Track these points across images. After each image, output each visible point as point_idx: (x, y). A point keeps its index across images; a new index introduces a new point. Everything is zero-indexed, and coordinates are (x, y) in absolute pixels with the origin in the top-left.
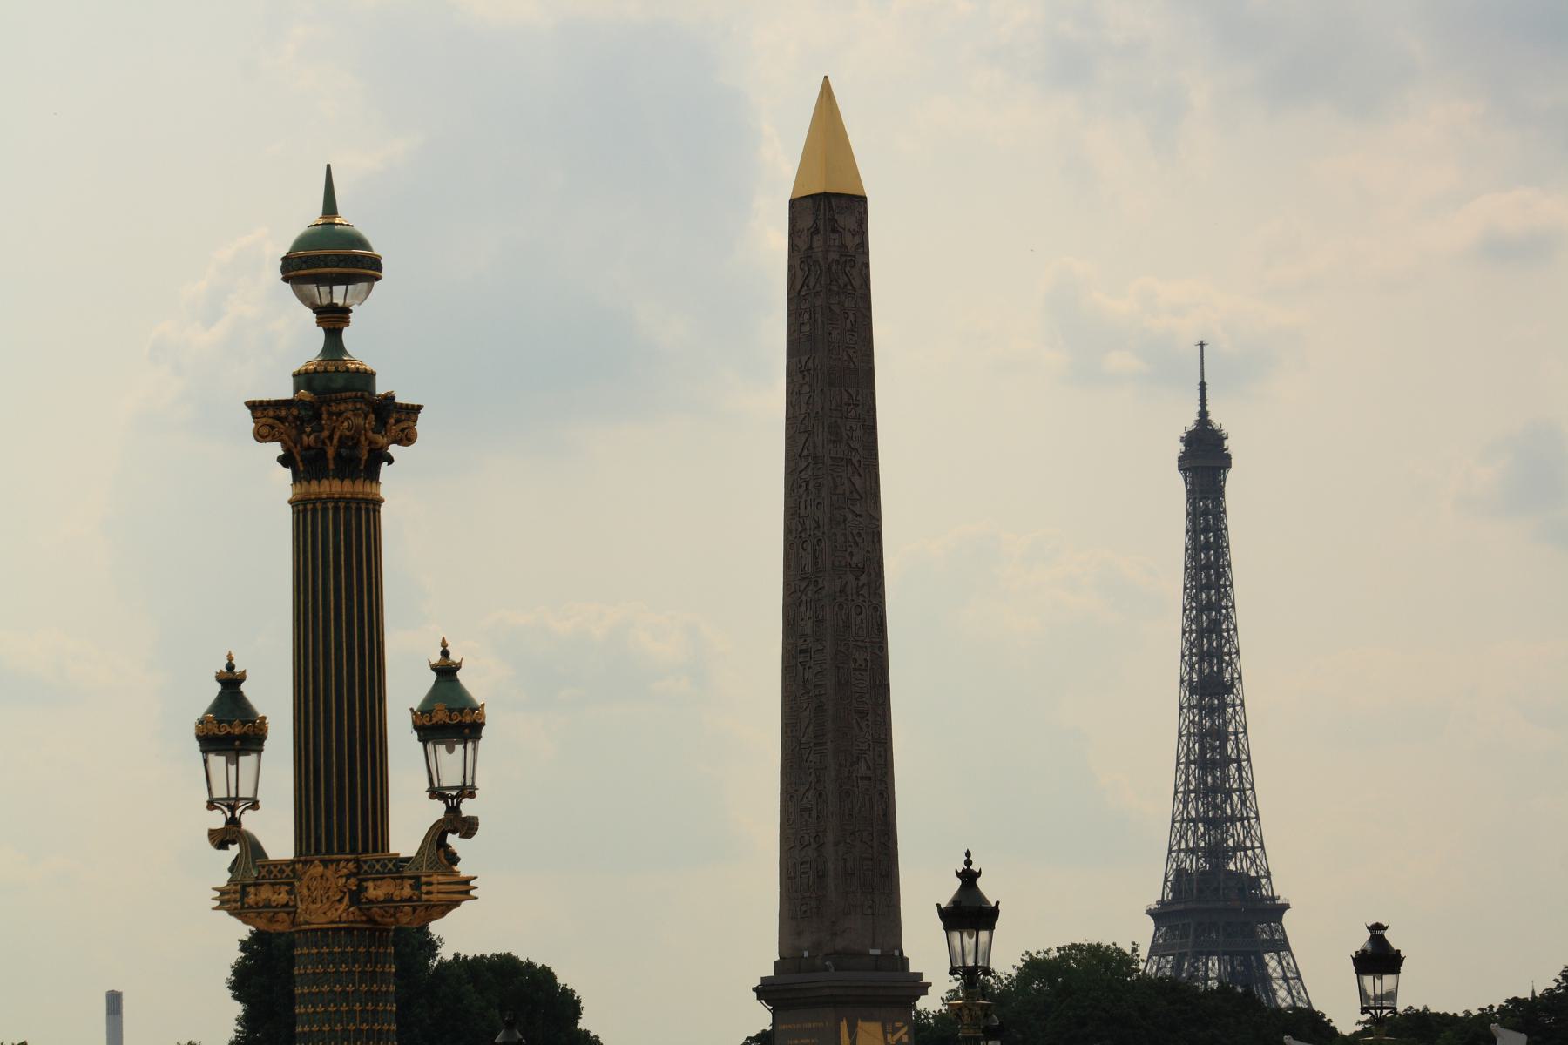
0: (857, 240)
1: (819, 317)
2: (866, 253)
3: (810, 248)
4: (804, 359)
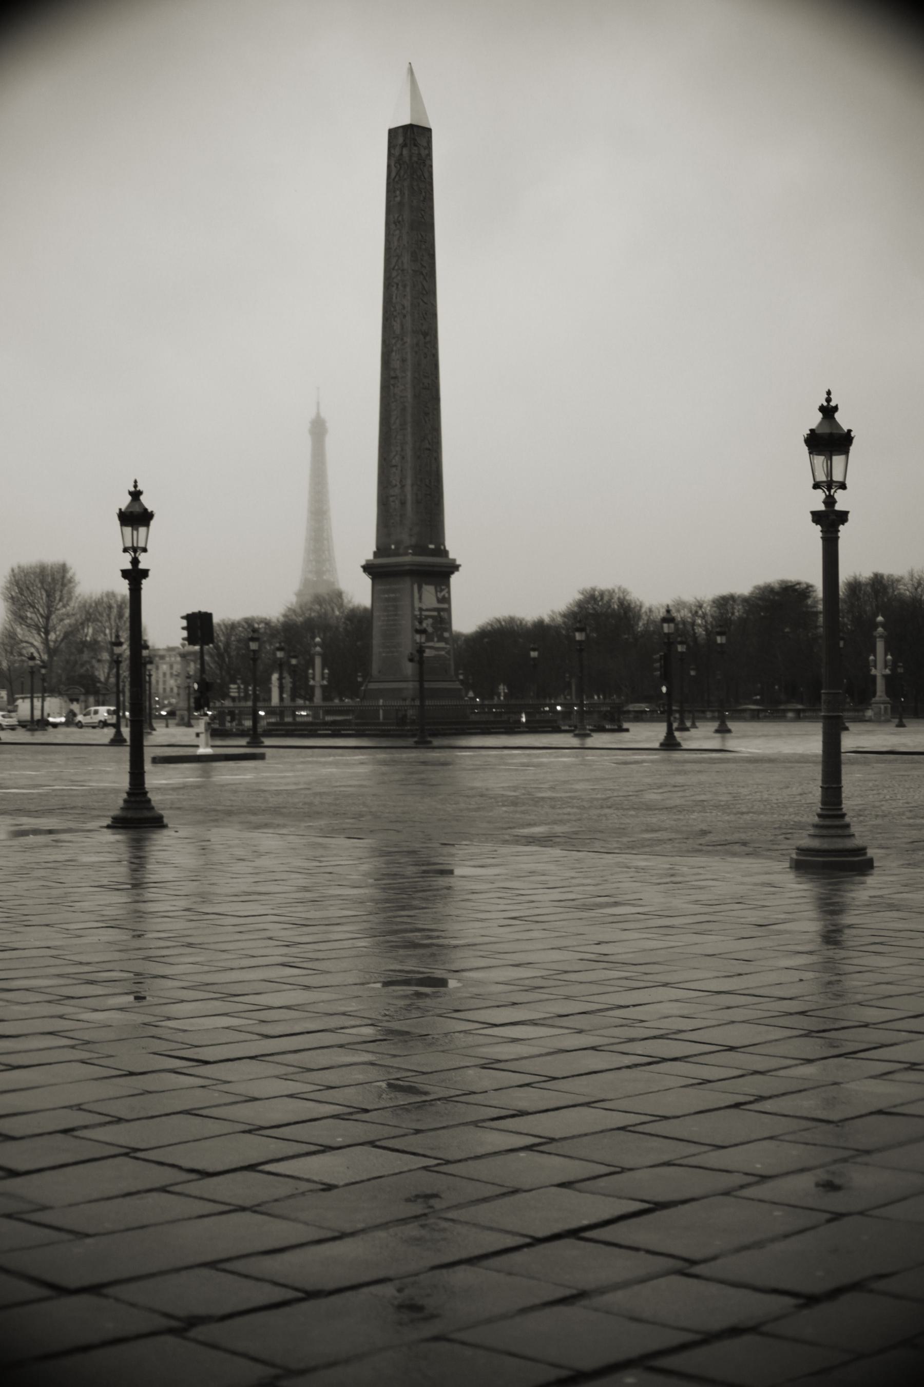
0: (427, 152)
1: (406, 192)
2: (431, 160)
3: (401, 154)
4: (396, 216)
